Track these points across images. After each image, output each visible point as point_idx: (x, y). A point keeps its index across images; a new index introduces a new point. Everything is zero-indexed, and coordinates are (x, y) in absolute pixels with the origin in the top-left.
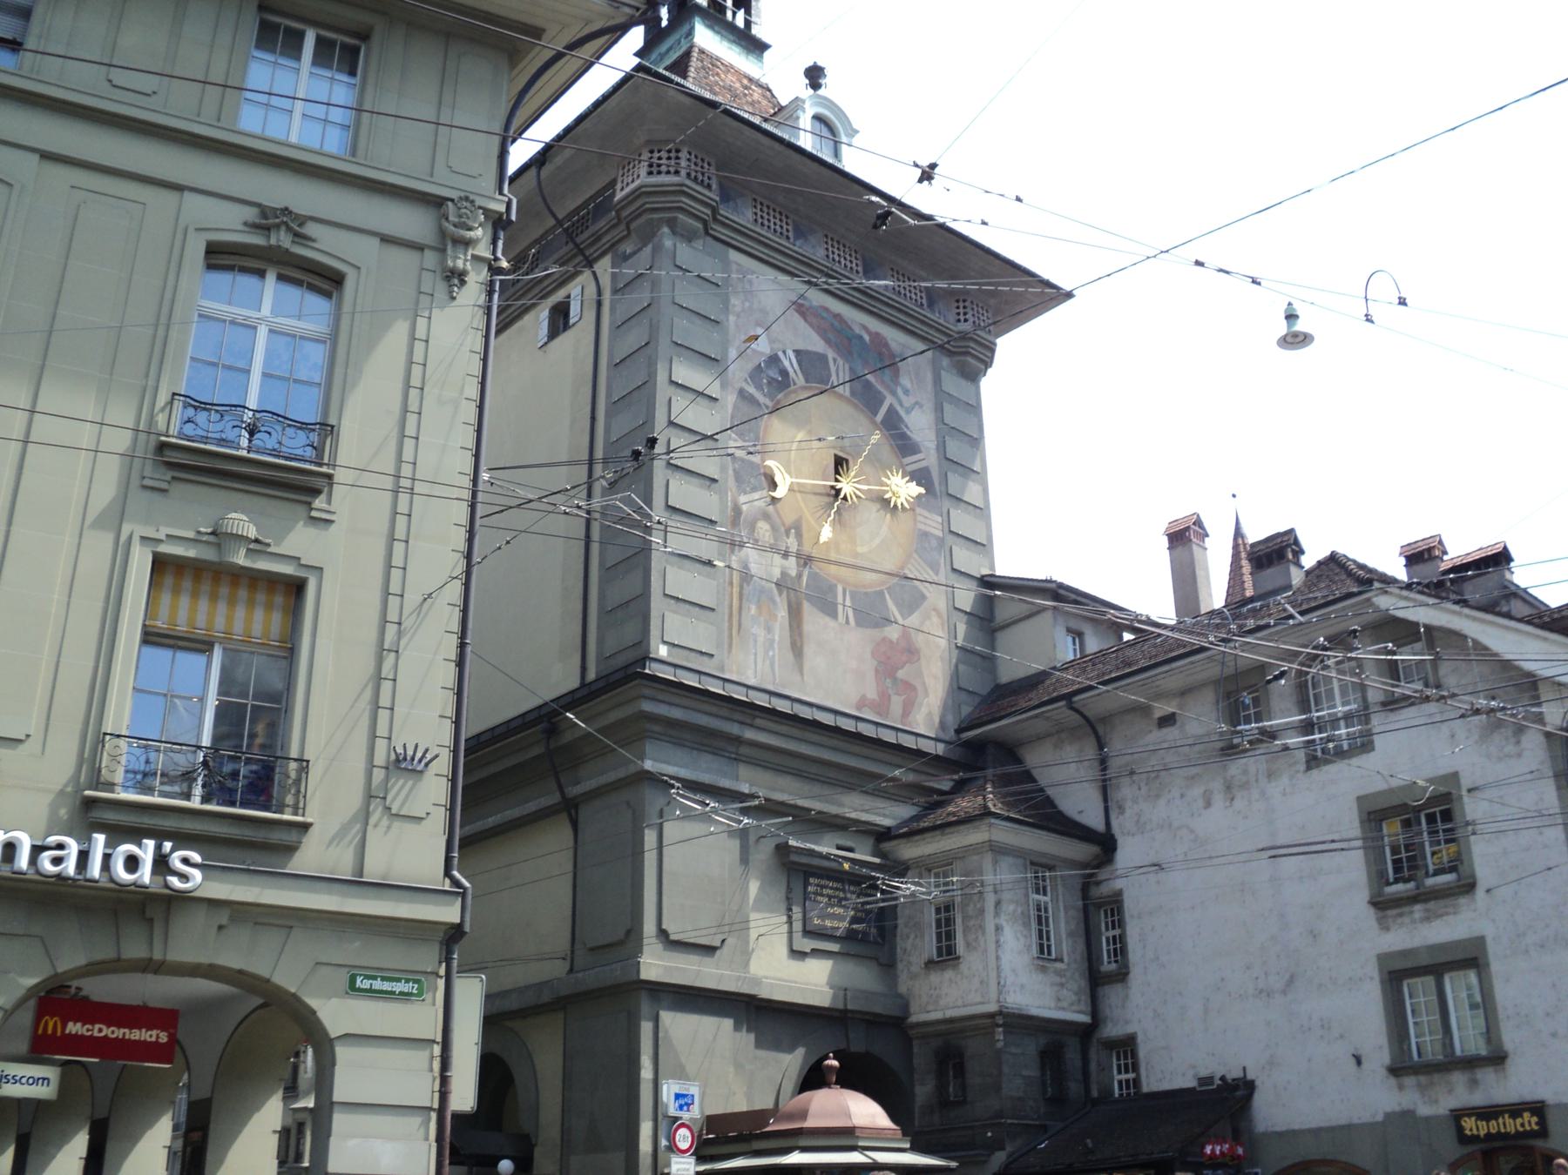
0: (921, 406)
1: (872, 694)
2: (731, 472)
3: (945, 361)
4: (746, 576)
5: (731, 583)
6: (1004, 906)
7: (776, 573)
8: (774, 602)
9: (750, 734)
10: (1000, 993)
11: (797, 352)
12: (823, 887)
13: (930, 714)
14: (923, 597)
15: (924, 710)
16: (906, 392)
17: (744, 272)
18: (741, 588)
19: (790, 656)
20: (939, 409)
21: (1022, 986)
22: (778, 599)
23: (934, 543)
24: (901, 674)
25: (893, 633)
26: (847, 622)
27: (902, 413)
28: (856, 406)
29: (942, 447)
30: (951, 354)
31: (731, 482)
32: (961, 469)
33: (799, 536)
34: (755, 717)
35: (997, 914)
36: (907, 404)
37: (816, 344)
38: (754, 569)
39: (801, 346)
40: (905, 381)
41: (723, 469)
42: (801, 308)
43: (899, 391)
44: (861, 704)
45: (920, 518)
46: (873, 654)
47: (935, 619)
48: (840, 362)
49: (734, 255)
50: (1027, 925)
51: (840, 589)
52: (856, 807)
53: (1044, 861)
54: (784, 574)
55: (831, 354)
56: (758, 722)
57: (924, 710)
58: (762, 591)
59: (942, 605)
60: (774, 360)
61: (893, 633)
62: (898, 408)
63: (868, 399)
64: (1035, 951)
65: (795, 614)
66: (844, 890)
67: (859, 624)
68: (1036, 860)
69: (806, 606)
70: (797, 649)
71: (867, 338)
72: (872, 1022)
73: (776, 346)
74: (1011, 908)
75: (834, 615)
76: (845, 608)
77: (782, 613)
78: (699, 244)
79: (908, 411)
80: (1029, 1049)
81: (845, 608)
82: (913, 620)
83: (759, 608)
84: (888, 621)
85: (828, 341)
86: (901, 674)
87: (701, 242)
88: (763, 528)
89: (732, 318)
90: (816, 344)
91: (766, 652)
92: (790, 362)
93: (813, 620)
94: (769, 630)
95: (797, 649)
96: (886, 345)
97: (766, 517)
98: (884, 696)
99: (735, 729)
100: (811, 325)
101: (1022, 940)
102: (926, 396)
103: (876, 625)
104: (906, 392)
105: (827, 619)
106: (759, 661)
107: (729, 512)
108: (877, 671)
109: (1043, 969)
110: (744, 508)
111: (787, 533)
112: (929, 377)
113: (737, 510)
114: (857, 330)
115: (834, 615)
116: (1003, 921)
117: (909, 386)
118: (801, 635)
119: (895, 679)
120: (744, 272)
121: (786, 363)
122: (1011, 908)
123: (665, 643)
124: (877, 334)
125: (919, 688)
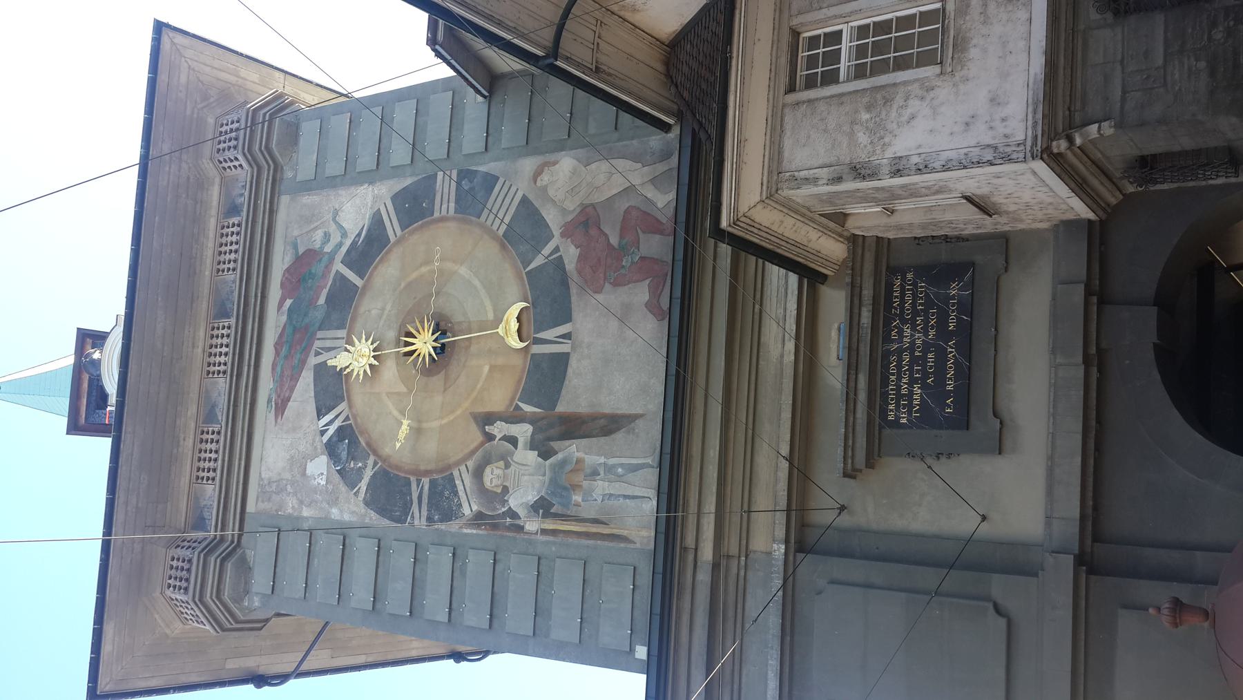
0: (336, 213)
1: (640, 293)
2: (442, 526)
4: (542, 507)
5: (554, 532)
6: (862, 156)
7: (532, 457)
8: (564, 462)
9: (707, 553)
10: (1008, 159)
11: (320, 414)
12: (899, 396)
13: (654, 181)
14: (525, 201)
15: (650, 192)
16: (327, 238)
18: (556, 516)
19: (619, 436)
20: (334, 183)
21: (994, 101)
22: (560, 456)
23: (466, 185)
24: (614, 241)
25: (571, 255)
26: (567, 336)
27: (348, 242)
28: (354, 320)
29: (369, 177)
30: (277, 168)
31: (453, 526)
32: (384, 141)
33: (487, 419)
34: (684, 549)
35: (873, 175)
36: (336, 238)
38: (532, 497)
39: (311, 407)
42: (280, 407)
43: (328, 249)
45: (444, 212)
46: (598, 290)
47: (545, 178)
48: (318, 344)
49: (251, 508)
50: (885, 96)
51: (537, 349)
52: (778, 344)
53: (784, 60)
54: (533, 446)
55: (313, 361)
56: (690, 541)
57: (650, 192)
58: (554, 482)
59: (528, 164)
60: (331, 449)
61: (571, 255)
62: (344, 249)
64: (930, 71)
65: (575, 427)
66: (900, 352)
67: (567, 318)
68: (784, 80)
69: (561, 408)
70: (608, 425)
71: (289, 302)
72: (1100, 294)
73: (320, 447)
74: (863, 138)
75: (563, 359)
76: (552, 340)
77: (573, 449)
78: (250, 554)
79: (344, 235)
81: (552, 340)
82: (553, 219)
83: (575, 487)
84: (559, 264)
85: (303, 362)
86: (614, 241)
87: (248, 551)
89: (306, 513)
91: (620, 478)
92: (332, 422)
93: (577, 397)
94: (595, 473)
95: (608, 425)
96: (288, 270)
97: (478, 474)
98: (646, 267)
99: (704, 576)
100: (292, 389)
101: (914, 104)
103: (564, 282)
104: (327, 238)
105: (570, 371)
106: (630, 491)
108: (616, 284)
109: (961, 45)
110: (475, 508)
111: (490, 437)
112: (307, 199)
114: (284, 318)
115: (563, 359)
116: (883, 159)
117: (319, 235)
118: (594, 417)
119: (622, 251)
120: (264, 495)
121: (332, 430)
122: (863, 138)
123: (632, 650)
124: (282, 285)
125: (623, 205)
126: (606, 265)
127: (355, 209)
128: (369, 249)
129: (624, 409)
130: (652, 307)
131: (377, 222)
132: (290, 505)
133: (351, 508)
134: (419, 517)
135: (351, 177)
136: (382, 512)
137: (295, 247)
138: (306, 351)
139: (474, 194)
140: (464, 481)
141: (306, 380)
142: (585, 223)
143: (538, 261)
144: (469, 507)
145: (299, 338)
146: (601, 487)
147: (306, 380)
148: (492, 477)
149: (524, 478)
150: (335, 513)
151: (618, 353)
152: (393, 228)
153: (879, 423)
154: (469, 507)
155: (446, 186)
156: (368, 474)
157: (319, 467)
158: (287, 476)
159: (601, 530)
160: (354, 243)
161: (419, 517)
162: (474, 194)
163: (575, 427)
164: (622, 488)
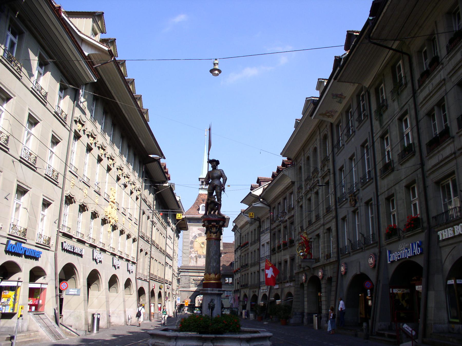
4: (191, 257)
17: (192, 228)
37: (200, 232)
42: (198, 229)
65: (196, 259)
70: (196, 262)
92: (197, 235)
95: (196, 262)
133: (191, 238)
134: (190, 246)
140: (193, 250)
144: (191, 250)
148: (193, 252)
149: (193, 255)
154: (191, 250)
157: (194, 235)
159: (190, 261)
161: (190, 246)
163: (196, 259)
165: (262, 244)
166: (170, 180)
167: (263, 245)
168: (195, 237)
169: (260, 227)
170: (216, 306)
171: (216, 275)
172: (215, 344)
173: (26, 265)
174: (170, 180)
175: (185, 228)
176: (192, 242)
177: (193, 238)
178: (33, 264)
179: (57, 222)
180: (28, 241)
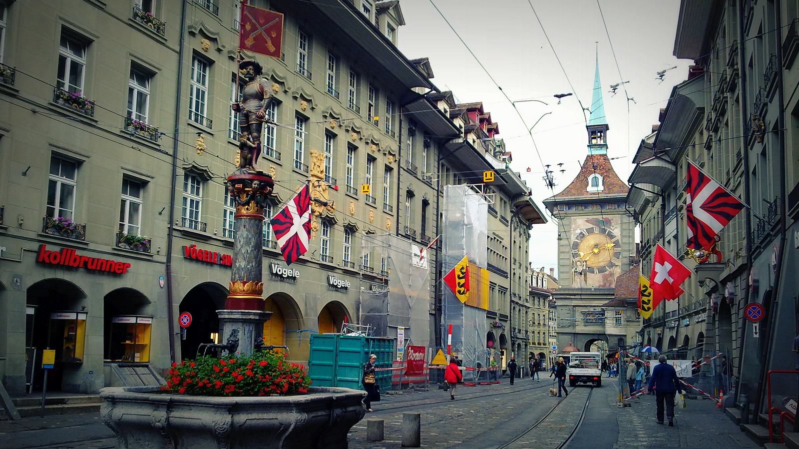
1: (602, 284)
3: (624, 215)
19: (584, 282)
20: (621, 227)
25: (607, 273)
31: (572, 258)
36: (613, 229)
37: (591, 226)
40: (613, 224)
41: (570, 256)
44: (599, 287)
55: (594, 226)
59: (620, 264)
60: (581, 233)
63: (603, 231)
69: (588, 273)
76: (596, 271)
79: (613, 230)
80: (616, 338)
81: (596, 271)
88: (578, 263)
90: (591, 226)
95: (586, 281)
97: (579, 261)
98: (605, 284)
102: (619, 227)
103: (603, 272)
107: (572, 263)
113: (573, 262)
121: (584, 233)
126: (605, 278)
127: (617, 232)
128: (611, 236)
129: (588, 282)
130: (600, 285)
131: (615, 237)
132: (573, 226)
133: (573, 239)
134: (573, 251)
135: (622, 230)
136: (573, 245)
137: (612, 220)
138: (596, 225)
139: (617, 255)
140: (577, 259)
141: (591, 226)
142: (611, 274)
143: (606, 267)
145: (597, 223)
146: (578, 280)
147: (591, 226)
148: (578, 263)
150: (572, 235)
151: (594, 281)
152: (614, 240)
153: (589, 314)
155: (619, 249)
156: (578, 241)
157: (579, 231)
158: (577, 224)
159: (573, 280)
160: (611, 232)
162: (617, 255)
163: (585, 275)
164: (578, 283)
165: (667, 240)
166: (497, 132)
167: (669, 242)
168: (582, 236)
169: (663, 207)
170: (240, 342)
171: (244, 283)
172: (172, 414)
173: (95, 290)
174: (497, 132)
175: (540, 218)
176: (576, 246)
177: (577, 238)
178: (110, 285)
179: (166, 213)
180: (92, 246)
